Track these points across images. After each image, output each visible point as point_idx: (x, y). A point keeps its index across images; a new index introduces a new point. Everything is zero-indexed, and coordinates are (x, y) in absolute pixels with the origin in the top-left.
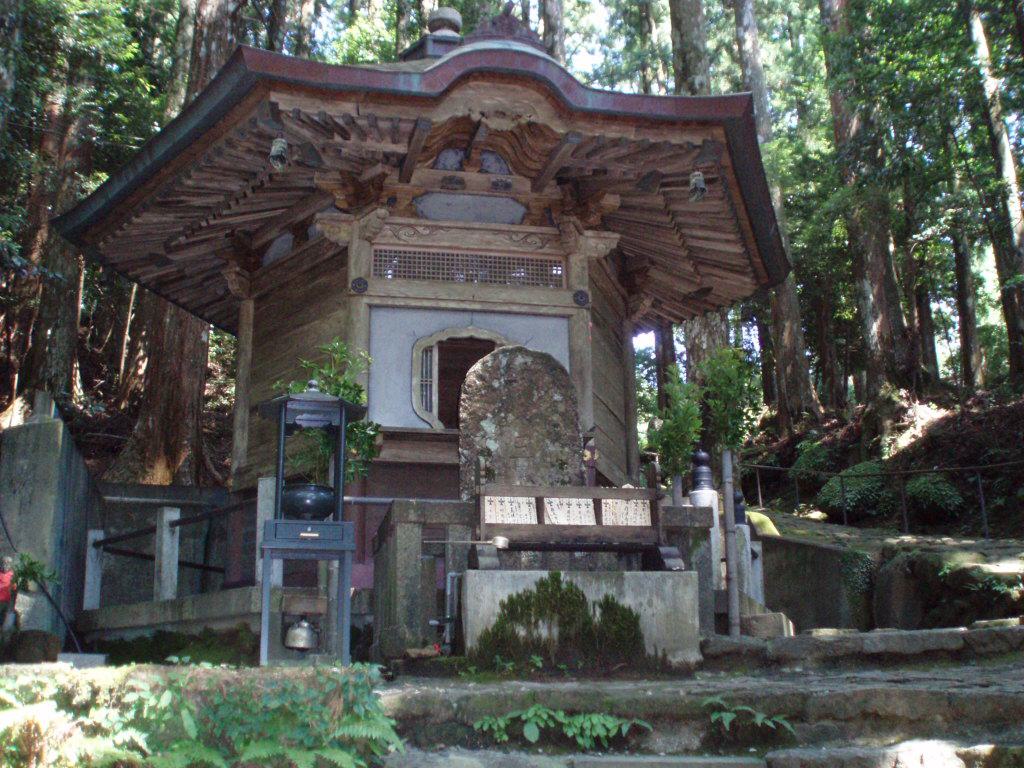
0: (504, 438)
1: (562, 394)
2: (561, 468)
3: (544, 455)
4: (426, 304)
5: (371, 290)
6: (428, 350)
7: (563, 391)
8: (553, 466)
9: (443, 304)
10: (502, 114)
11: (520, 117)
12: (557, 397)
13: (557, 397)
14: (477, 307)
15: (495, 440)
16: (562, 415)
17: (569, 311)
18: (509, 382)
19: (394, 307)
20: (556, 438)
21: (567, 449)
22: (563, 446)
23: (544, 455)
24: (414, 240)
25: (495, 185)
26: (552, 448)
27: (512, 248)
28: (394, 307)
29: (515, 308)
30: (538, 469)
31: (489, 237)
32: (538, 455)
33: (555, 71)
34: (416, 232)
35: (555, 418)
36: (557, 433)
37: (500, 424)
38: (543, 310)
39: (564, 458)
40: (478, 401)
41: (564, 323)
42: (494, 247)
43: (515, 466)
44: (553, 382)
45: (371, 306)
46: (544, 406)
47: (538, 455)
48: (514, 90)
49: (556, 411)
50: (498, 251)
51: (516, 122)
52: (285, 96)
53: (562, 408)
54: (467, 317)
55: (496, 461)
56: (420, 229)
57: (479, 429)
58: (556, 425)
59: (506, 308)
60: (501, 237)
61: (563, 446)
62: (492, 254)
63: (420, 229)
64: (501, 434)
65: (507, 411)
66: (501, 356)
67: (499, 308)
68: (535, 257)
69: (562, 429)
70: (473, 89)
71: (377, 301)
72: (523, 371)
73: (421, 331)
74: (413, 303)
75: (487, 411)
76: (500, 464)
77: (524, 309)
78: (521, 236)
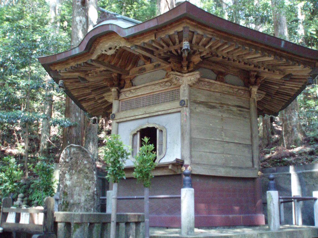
0: (72, 180)
1: (87, 161)
2: (89, 190)
3: (84, 185)
5: (116, 118)
6: (134, 135)
7: (87, 159)
8: (87, 189)
9: (137, 117)
10: (110, 49)
11: (116, 47)
12: (86, 162)
13: (86, 162)
16: (88, 169)
17: (179, 110)
18: (71, 159)
20: (87, 178)
21: (91, 182)
22: (90, 181)
23: (84, 185)
24: (131, 95)
25: (155, 66)
26: (86, 182)
29: (160, 113)
31: (153, 87)
32: (82, 185)
33: (115, 27)
34: (131, 92)
35: (86, 170)
36: (87, 176)
37: (71, 175)
38: (169, 111)
39: (90, 186)
40: (63, 167)
41: (179, 114)
45: (118, 123)
46: (82, 166)
47: (82, 185)
49: (86, 168)
51: (115, 49)
52: (58, 67)
53: (88, 166)
54: (147, 120)
56: (132, 91)
57: (64, 177)
58: (87, 173)
59: (157, 114)
60: (157, 86)
61: (90, 181)
62: (156, 93)
63: (132, 91)
65: (73, 170)
66: (67, 149)
67: (155, 114)
68: (170, 90)
69: (89, 175)
70: (102, 43)
71: (118, 121)
72: (74, 154)
74: (128, 119)
76: (70, 190)
77: (163, 113)
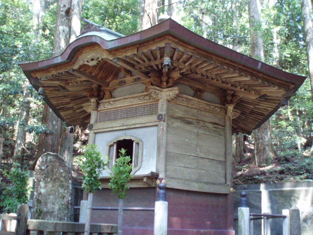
0: (47, 188)
1: (63, 170)
2: (63, 199)
3: (59, 193)
4: (109, 129)
5: (94, 128)
6: (111, 146)
7: (63, 168)
8: (61, 198)
9: (114, 129)
10: (92, 60)
11: (98, 58)
12: (62, 171)
13: (62, 171)
14: (125, 127)
15: (44, 189)
16: (64, 177)
17: (156, 123)
18: (47, 166)
19: (147, 127)
20: (62, 186)
21: (66, 191)
22: (65, 190)
23: (59, 193)
24: (110, 107)
25: (135, 80)
26: (61, 190)
27: (139, 102)
28: (147, 127)
29: (137, 126)
30: (56, 200)
31: (132, 100)
32: (57, 194)
33: (98, 39)
34: (110, 103)
35: (62, 179)
36: (63, 185)
37: (46, 183)
38: (147, 125)
39: (64, 195)
40: (39, 175)
41: (156, 128)
42: (134, 104)
43: (49, 198)
44: (60, 165)
45: (96, 133)
46: (58, 174)
47: (57, 194)
48: (96, 49)
49: (62, 177)
50: (136, 105)
51: (97, 61)
52: (39, 74)
53: (63, 175)
54: (124, 131)
55: (43, 197)
56: (111, 102)
57: (39, 185)
58: (62, 182)
59: (134, 126)
60: (136, 99)
61: (65, 190)
62: (135, 106)
63: (111, 102)
64: (46, 187)
65: (48, 178)
66: (44, 157)
67: (132, 127)
68: (148, 104)
69: (64, 183)
70: (84, 53)
71: (96, 131)
72: (50, 162)
73: (109, 140)
74: (106, 130)
75: (41, 178)
76: (44, 198)
77: (140, 126)
78: (143, 97)
